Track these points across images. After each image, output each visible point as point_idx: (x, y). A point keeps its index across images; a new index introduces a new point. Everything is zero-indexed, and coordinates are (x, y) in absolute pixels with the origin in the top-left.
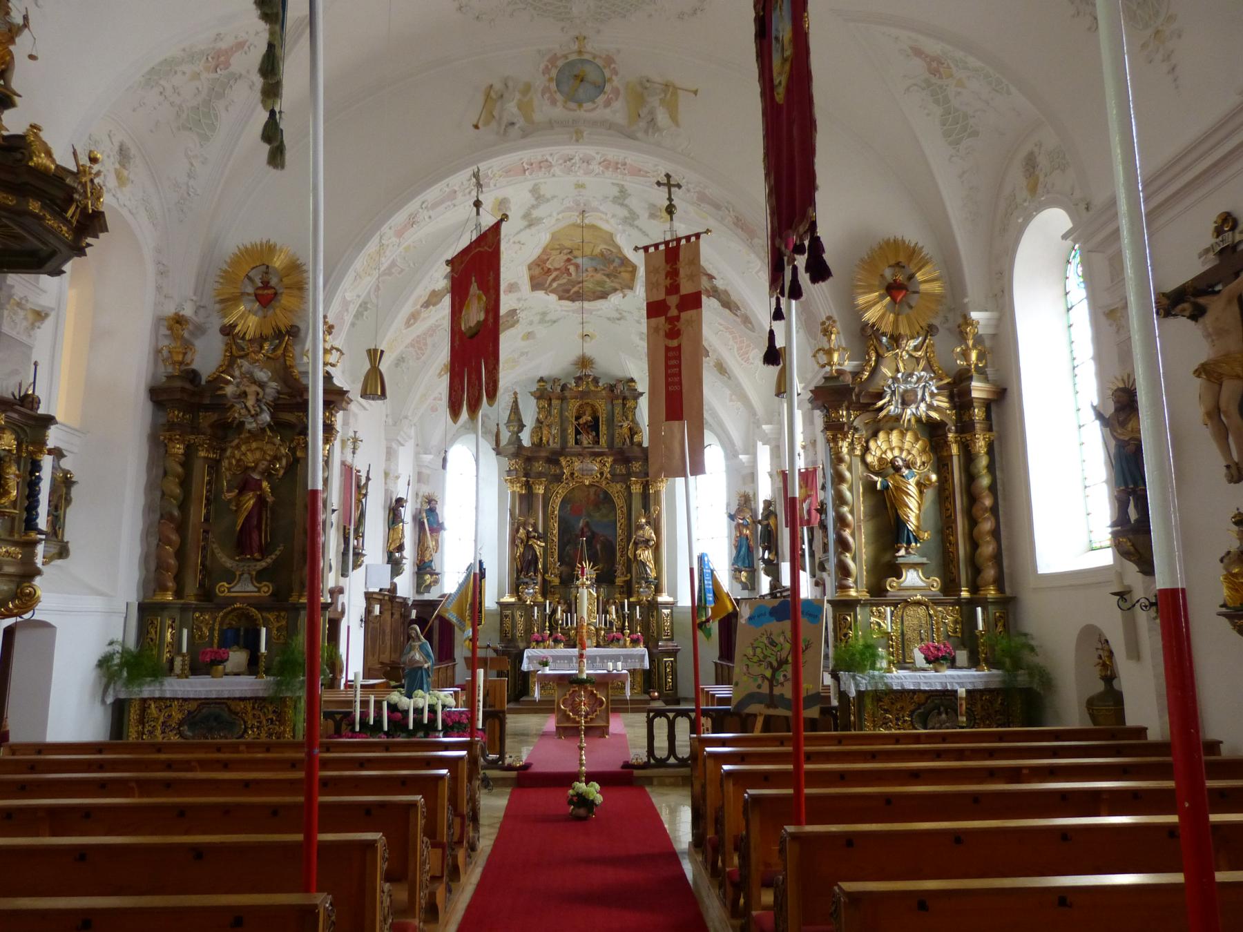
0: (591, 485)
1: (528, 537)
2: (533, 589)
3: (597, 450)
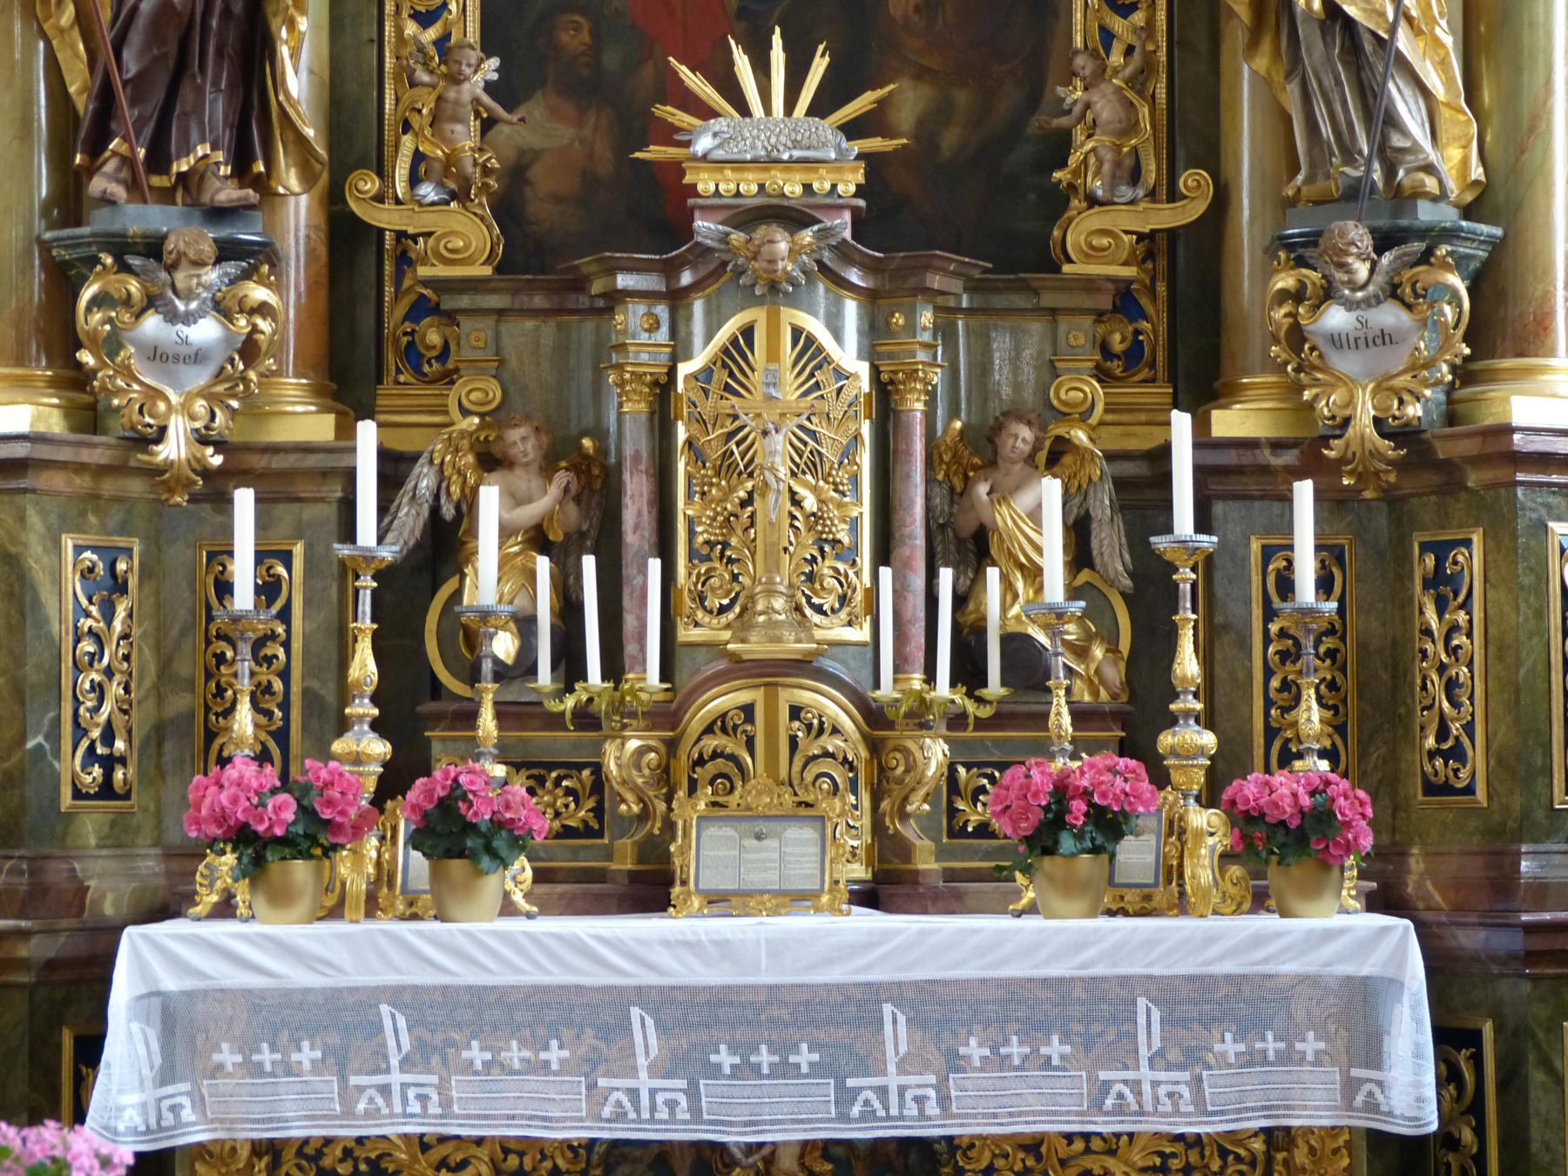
2: (222, 309)
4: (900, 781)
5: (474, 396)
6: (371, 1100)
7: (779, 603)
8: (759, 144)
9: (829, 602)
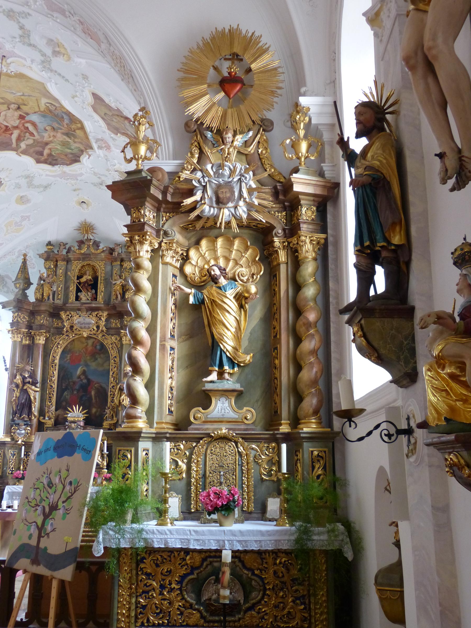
0: (89, 338)
1: (24, 383)
2: (25, 430)
3: (94, 305)
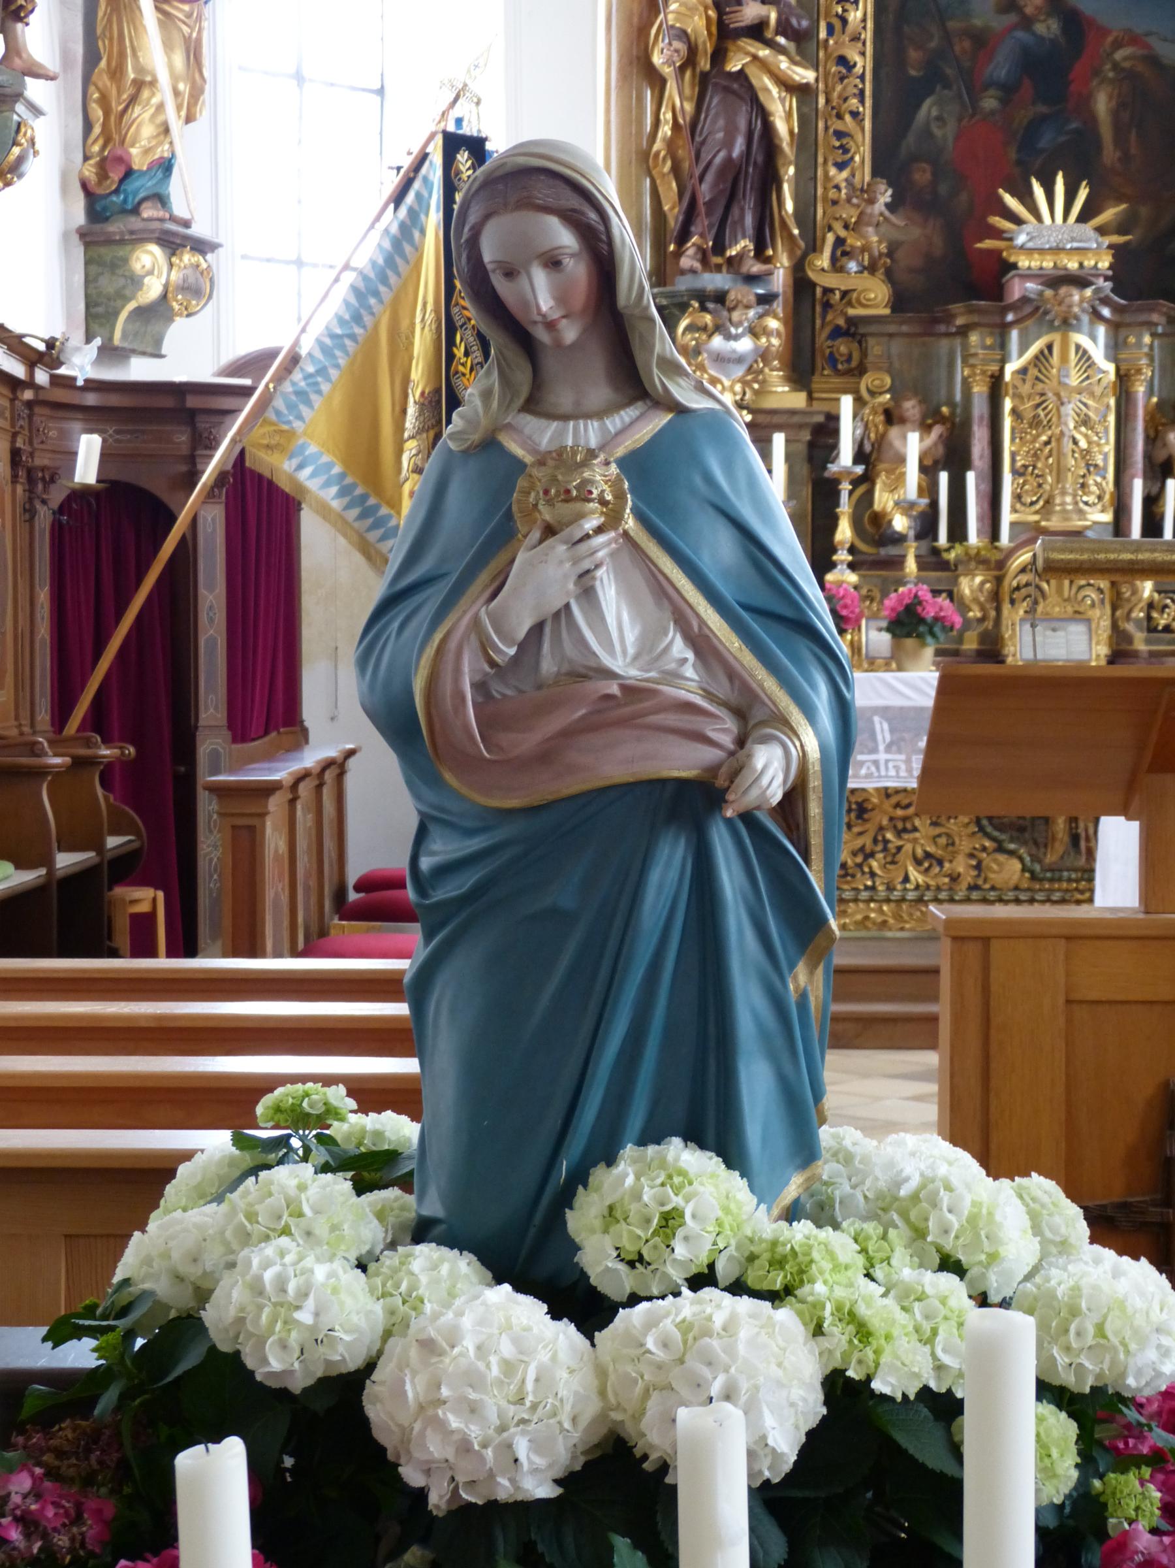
2: (754, 332)
4: (1128, 600)
5: (877, 382)
6: (868, 768)
7: (1069, 499)
8: (1052, 239)
9: (1091, 499)
